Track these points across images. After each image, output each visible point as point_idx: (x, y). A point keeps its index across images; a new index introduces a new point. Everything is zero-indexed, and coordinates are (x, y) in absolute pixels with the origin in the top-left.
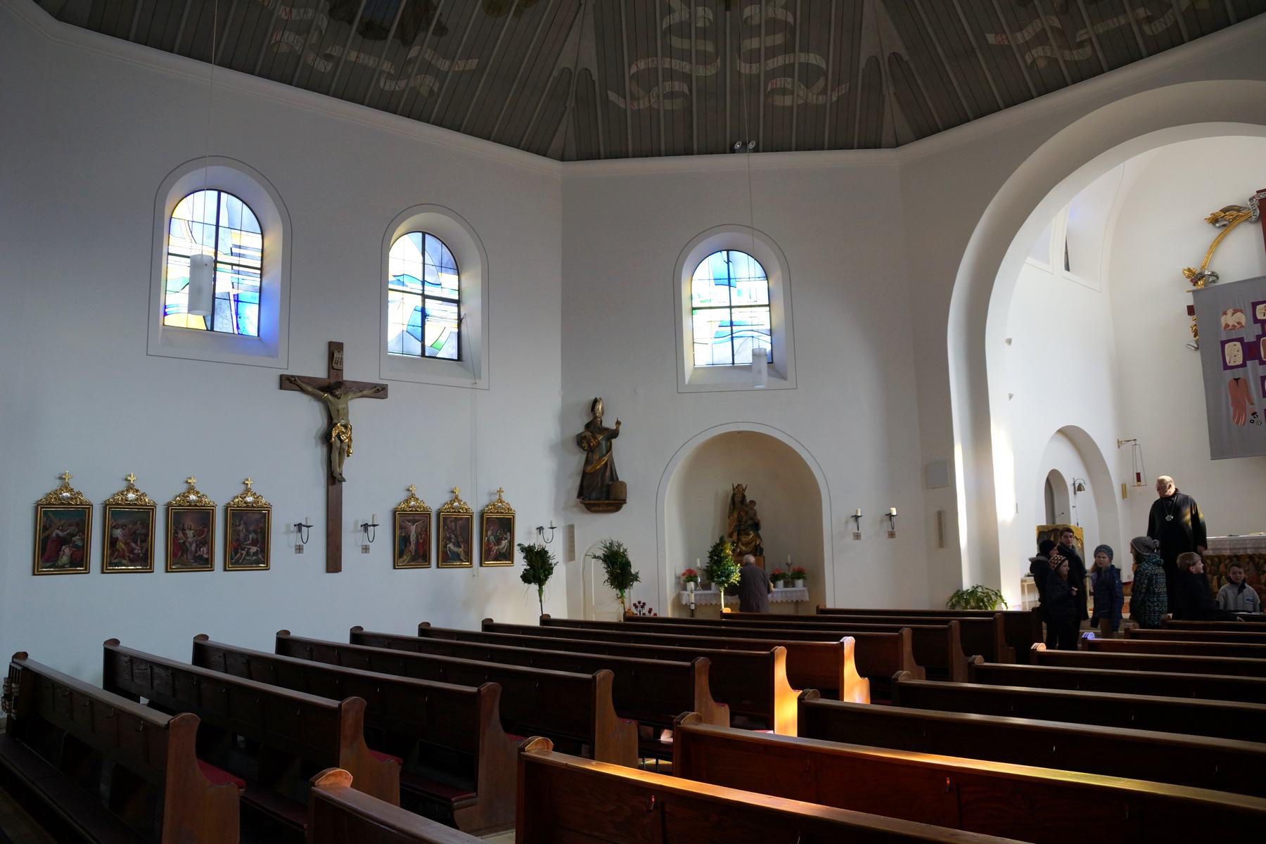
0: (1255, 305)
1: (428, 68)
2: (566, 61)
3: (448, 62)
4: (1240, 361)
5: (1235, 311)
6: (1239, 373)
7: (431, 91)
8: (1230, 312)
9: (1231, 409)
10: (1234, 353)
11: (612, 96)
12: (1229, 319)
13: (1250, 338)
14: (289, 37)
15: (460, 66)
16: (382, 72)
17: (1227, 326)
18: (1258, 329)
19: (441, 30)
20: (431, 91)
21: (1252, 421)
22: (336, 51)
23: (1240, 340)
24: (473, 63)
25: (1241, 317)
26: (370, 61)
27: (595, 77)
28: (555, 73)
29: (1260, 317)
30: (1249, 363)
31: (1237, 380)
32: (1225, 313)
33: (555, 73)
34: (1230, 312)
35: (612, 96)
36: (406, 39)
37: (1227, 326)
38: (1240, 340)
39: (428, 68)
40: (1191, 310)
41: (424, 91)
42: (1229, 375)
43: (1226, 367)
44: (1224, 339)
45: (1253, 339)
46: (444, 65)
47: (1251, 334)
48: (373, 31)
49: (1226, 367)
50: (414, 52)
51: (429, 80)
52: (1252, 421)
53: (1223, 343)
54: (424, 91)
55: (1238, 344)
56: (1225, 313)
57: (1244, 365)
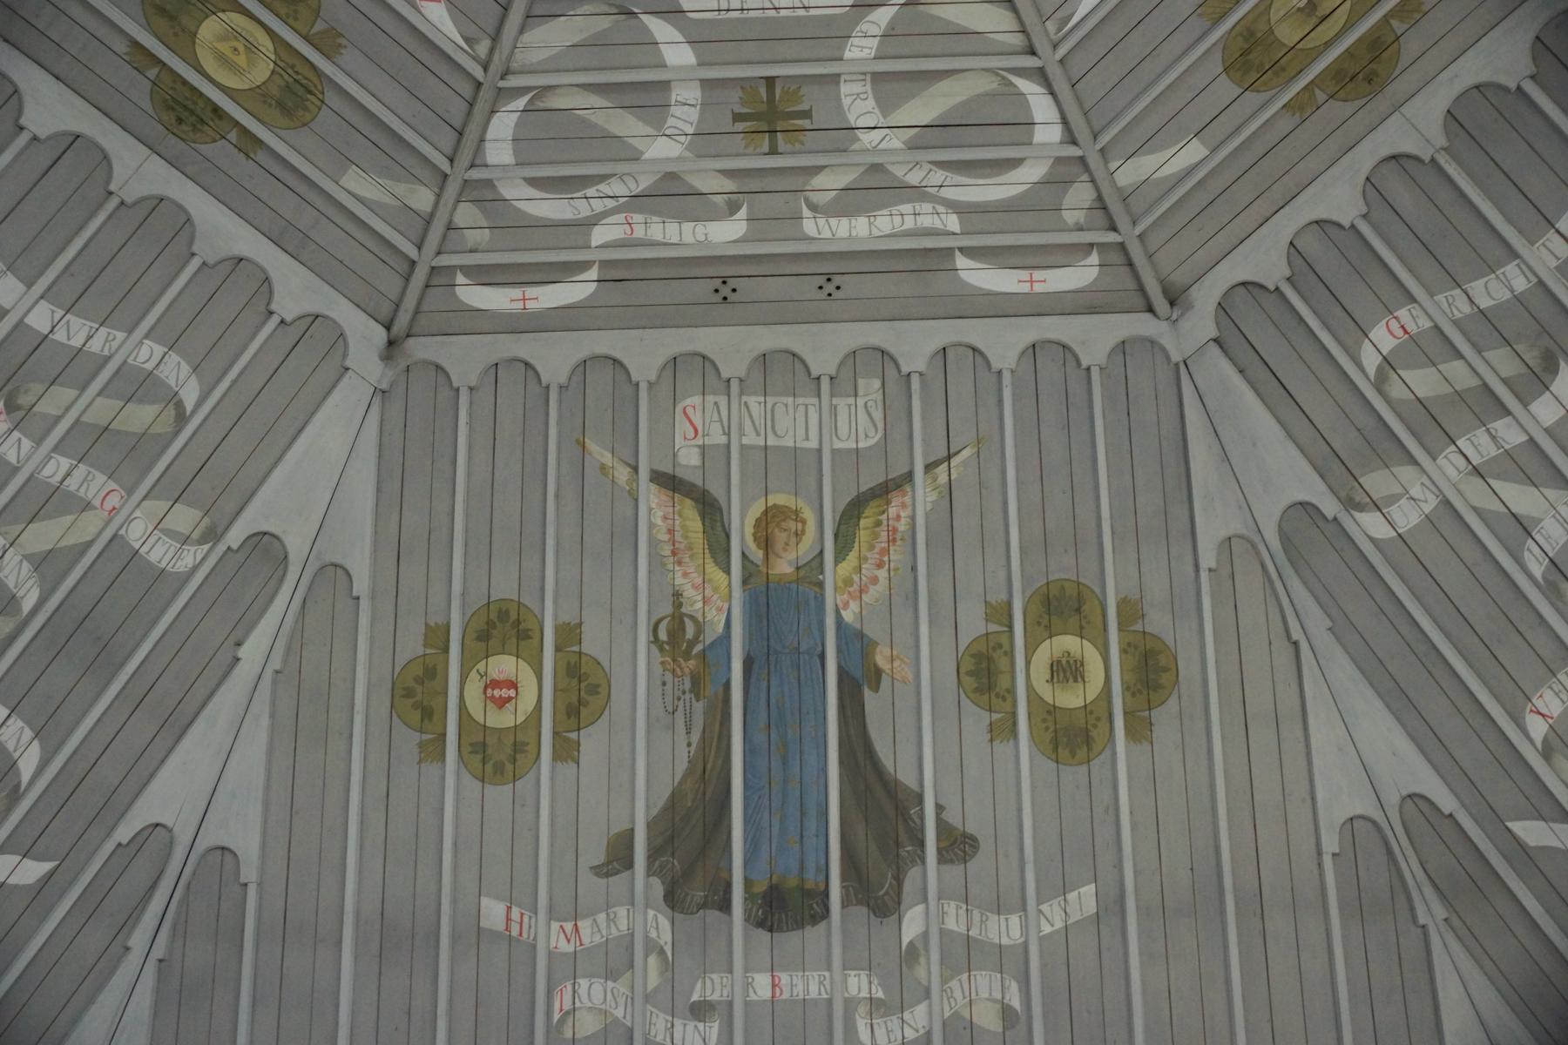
1: (965, 954)
2: (1342, 797)
3: (1015, 920)
7: (1007, 1013)
11: (1532, 832)
14: (592, 991)
15: (1052, 918)
16: (850, 1005)
19: (958, 846)
20: (1007, 1013)
22: (713, 988)
24: (1084, 899)
26: (808, 985)
27: (1447, 803)
28: (1330, 844)
33: (1330, 844)
35: (1532, 832)
36: (877, 896)
39: (965, 954)
41: (988, 1019)
46: (1007, 930)
48: (785, 908)
50: (912, 923)
51: (986, 983)
54: (988, 1019)
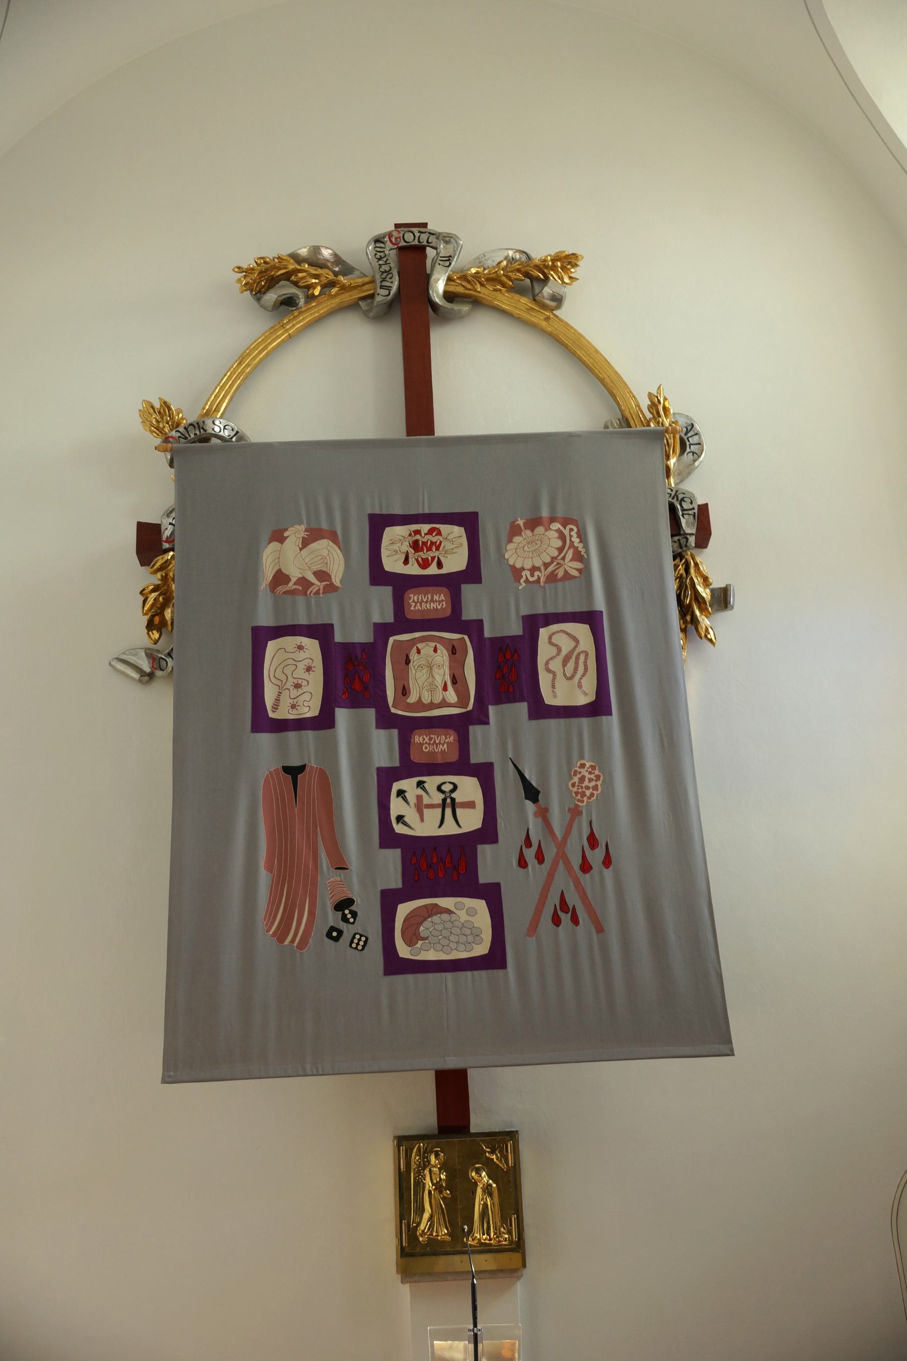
0: (379, 524)
4: (311, 708)
5: (313, 536)
6: (304, 748)
8: (295, 534)
9: (264, 878)
10: (295, 676)
12: (292, 557)
13: (357, 632)
17: (280, 578)
18: (380, 605)
21: (335, 935)
23: (321, 633)
25: (330, 557)
29: (392, 563)
30: (342, 715)
31: (294, 772)
32: (279, 537)
34: (295, 534)
37: (280, 578)
38: (321, 633)
40: (149, 541)
42: (266, 752)
43: (262, 722)
44: (265, 619)
45: (361, 635)
47: (359, 615)
49: (262, 722)
52: (335, 935)
53: (261, 637)
55: (312, 646)
56: (279, 537)
57: (324, 721)
